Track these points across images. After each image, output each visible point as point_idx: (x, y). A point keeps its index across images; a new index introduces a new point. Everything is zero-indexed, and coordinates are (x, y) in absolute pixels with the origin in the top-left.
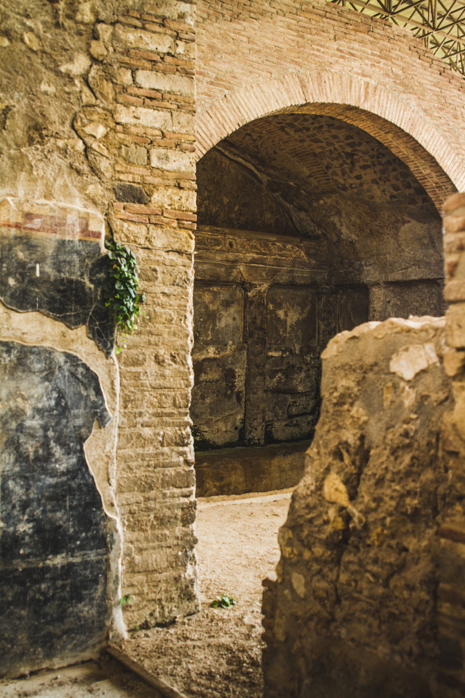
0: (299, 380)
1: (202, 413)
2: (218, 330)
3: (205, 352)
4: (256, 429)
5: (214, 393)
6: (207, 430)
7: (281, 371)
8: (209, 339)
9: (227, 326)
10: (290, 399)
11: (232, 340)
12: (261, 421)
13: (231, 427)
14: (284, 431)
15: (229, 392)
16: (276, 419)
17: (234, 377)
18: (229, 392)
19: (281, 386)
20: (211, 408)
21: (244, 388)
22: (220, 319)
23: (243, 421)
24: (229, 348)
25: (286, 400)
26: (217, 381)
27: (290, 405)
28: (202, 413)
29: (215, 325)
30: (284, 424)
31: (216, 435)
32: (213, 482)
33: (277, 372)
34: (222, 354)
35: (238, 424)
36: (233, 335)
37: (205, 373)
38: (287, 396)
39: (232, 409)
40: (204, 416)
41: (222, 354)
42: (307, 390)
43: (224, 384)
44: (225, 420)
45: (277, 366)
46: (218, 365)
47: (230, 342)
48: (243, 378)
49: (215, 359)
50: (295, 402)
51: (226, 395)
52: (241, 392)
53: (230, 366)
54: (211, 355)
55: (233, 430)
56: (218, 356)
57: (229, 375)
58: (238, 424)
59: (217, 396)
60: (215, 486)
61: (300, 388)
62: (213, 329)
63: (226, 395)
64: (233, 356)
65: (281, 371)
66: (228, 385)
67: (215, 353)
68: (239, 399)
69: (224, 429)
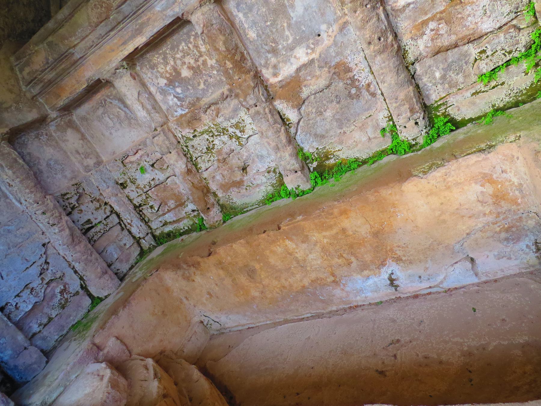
0: (480, 12)
1: (327, 131)
2: (296, 22)
3: (293, 60)
4: (405, 127)
5: (332, 101)
6: (340, 147)
7: (432, 19)
8: (290, 42)
9: (306, 9)
10: (473, 50)
11: (324, 22)
12: (409, 114)
13: (375, 131)
14: (474, 104)
15: (353, 91)
16: (455, 90)
17: (349, 70)
18: (353, 91)
19: (439, 43)
20: (339, 120)
21: (371, 77)
22: (292, 6)
23: (390, 118)
24: (324, 35)
25: (466, 55)
26: (328, 87)
27: (476, 60)
28: (327, 131)
29: (289, 18)
30: (468, 94)
31: (356, 149)
32: (319, 233)
33: (425, 23)
34: (319, 49)
35: (384, 124)
36: (323, 15)
37: (305, 86)
38: (466, 47)
39: (368, 109)
40: (332, 133)
41: (319, 49)
42: (504, 21)
43: (341, 84)
44: (362, 128)
45: (426, 14)
46: (320, 67)
47: (324, 27)
48: (363, 65)
49: (312, 61)
50: (484, 51)
51: (350, 96)
52: (369, 85)
53: (337, 60)
54: (304, 59)
55: (379, 133)
56: (314, 56)
57: (341, 70)
58: (384, 124)
59: (338, 103)
60: (324, 237)
61: (487, 26)
62: (289, 25)
63: (350, 96)
64: (335, 43)
65: (432, 19)
66: (346, 84)
67: (307, 53)
68: (373, 95)
69: (364, 139)
